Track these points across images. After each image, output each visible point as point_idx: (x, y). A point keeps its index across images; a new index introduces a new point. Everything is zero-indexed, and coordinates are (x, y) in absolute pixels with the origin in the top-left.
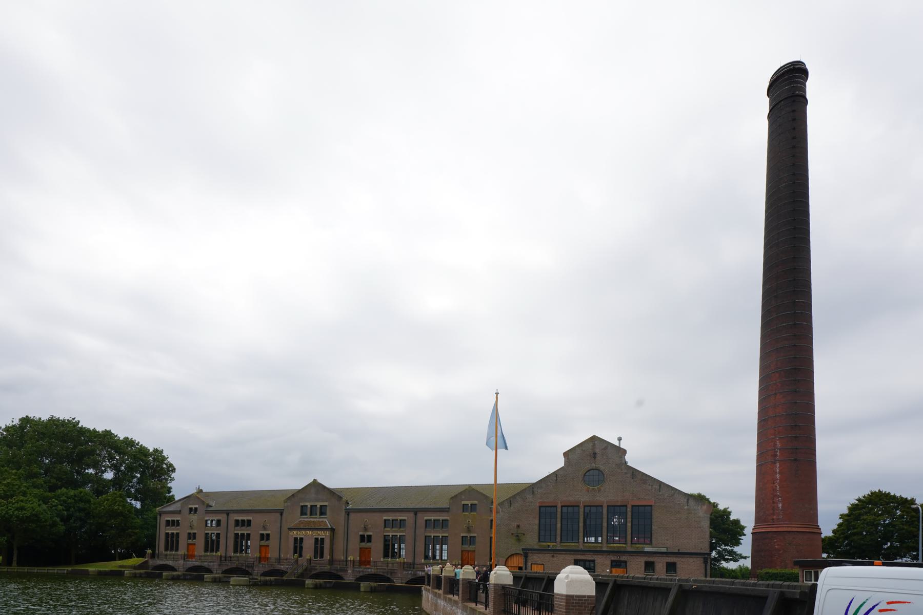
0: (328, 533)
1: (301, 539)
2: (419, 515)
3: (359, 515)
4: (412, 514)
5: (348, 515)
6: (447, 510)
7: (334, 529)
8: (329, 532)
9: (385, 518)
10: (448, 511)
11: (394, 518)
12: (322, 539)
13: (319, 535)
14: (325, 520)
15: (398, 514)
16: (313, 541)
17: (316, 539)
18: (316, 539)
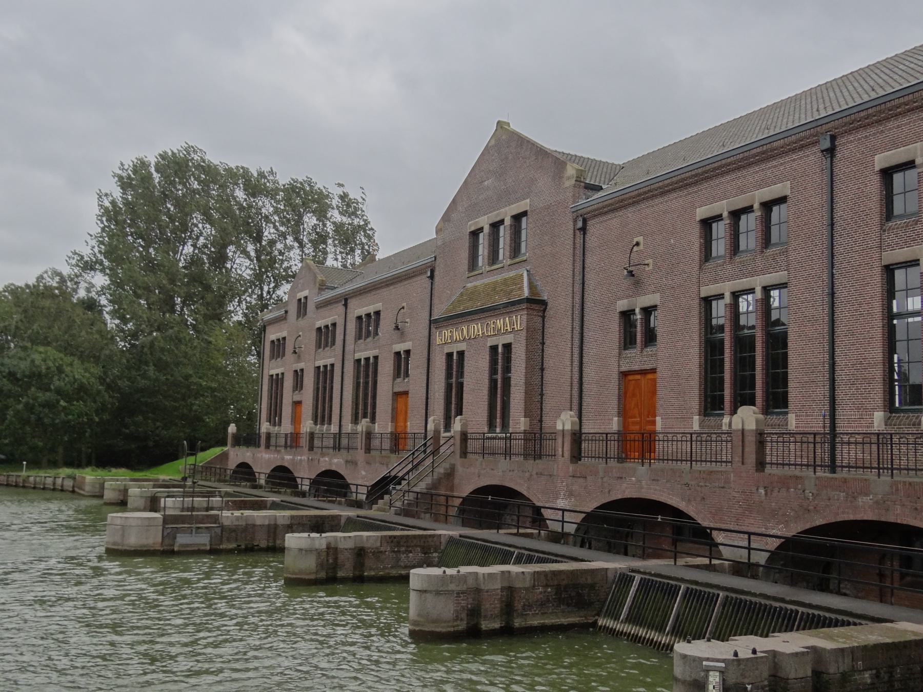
0: (519, 320)
1: (461, 354)
2: (848, 148)
3: (614, 221)
4: (812, 159)
5: (584, 230)
7: (544, 303)
8: (525, 317)
9: (703, 212)
11: (739, 202)
12: (508, 347)
13: (498, 333)
15: (752, 175)
16: (484, 362)
17: (494, 349)
18: (494, 349)
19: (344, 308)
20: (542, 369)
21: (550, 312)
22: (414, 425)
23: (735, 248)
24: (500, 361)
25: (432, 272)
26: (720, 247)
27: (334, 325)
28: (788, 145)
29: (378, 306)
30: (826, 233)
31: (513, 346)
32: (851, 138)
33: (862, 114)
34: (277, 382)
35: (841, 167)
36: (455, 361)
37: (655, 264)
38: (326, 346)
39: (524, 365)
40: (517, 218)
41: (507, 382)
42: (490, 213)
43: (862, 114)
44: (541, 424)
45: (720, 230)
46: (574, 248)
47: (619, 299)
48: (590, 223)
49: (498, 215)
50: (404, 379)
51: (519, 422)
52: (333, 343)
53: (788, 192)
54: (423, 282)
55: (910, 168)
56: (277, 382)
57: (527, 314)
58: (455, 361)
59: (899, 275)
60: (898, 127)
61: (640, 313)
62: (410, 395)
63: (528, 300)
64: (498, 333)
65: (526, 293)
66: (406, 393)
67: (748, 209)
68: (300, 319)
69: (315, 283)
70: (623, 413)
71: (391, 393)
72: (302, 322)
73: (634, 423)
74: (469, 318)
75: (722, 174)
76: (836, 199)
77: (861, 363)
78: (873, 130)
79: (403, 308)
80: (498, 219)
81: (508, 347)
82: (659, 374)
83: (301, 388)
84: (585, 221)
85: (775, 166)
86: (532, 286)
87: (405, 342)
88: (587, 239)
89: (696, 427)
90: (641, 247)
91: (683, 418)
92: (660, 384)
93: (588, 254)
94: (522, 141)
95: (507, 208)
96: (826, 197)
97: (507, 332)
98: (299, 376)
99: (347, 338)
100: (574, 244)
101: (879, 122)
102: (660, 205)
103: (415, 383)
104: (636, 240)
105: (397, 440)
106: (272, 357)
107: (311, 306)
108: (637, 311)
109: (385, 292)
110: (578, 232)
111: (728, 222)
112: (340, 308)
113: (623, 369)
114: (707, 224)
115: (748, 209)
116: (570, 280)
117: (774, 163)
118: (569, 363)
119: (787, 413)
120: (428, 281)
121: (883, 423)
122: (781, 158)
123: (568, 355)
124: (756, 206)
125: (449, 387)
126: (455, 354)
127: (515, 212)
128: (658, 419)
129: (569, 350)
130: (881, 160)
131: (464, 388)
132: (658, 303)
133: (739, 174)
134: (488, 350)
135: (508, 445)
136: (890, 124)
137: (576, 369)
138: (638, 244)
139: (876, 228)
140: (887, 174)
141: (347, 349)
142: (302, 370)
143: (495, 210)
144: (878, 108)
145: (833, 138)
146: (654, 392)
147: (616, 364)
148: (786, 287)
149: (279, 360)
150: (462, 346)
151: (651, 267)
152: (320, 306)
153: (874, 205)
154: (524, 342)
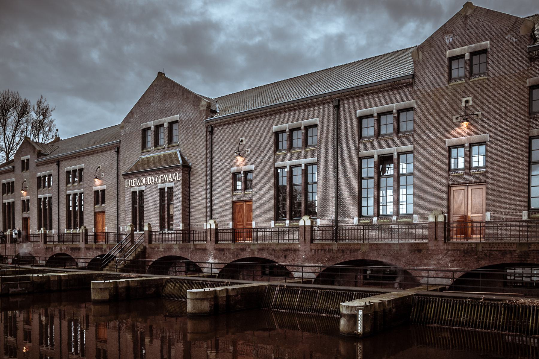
0: (177, 176)
1: (141, 192)
2: (346, 106)
3: (229, 129)
5: (212, 132)
7: (190, 167)
8: (181, 174)
9: (275, 128)
10: (412, 85)
11: (295, 124)
12: (171, 189)
14: (174, 151)
16: (156, 196)
17: (162, 190)
18: (162, 190)
19: (57, 166)
20: (189, 200)
23: (291, 147)
26: (284, 144)
28: (319, 102)
29: (82, 166)
31: (174, 188)
35: (342, 114)
39: (181, 198)
40: (171, 124)
42: (155, 120)
44: (189, 227)
45: (284, 138)
46: (206, 141)
47: (232, 167)
48: (215, 129)
49: (160, 121)
50: (101, 205)
51: (178, 225)
54: (113, 153)
55: (371, 117)
57: (182, 173)
59: (364, 162)
61: (243, 174)
62: (106, 213)
64: (165, 182)
65: (181, 163)
66: (104, 212)
67: (299, 129)
68: (24, 172)
69: (34, 152)
70: (234, 220)
72: (25, 174)
73: (240, 225)
77: (349, 197)
80: (160, 123)
83: (28, 210)
85: (312, 111)
89: (273, 226)
90: (244, 142)
91: (266, 222)
92: (254, 206)
93: (214, 145)
97: (170, 182)
99: (60, 182)
100: (206, 139)
101: (359, 96)
103: (110, 207)
104: (241, 139)
107: (32, 164)
108: (242, 172)
109: (87, 158)
111: (288, 134)
112: (55, 166)
113: (234, 200)
115: (299, 129)
116: (204, 157)
117: (311, 109)
118: (204, 197)
119: (316, 219)
121: (357, 222)
122: (315, 107)
123: (204, 193)
126: (138, 192)
127: (170, 121)
128: (254, 223)
129: (204, 191)
130: (359, 113)
133: (294, 112)
134: (159, 190)
136: (363, 98)
137: (209, 200)
138: (242, 141)
139: (357, 142)
140: (361, 119)
141: (61, 189)
143: (158, 119)
145: (339, 101)
148: (316, 164)
150: (143, 188)
151: (249, 152)
154: (180, 187)
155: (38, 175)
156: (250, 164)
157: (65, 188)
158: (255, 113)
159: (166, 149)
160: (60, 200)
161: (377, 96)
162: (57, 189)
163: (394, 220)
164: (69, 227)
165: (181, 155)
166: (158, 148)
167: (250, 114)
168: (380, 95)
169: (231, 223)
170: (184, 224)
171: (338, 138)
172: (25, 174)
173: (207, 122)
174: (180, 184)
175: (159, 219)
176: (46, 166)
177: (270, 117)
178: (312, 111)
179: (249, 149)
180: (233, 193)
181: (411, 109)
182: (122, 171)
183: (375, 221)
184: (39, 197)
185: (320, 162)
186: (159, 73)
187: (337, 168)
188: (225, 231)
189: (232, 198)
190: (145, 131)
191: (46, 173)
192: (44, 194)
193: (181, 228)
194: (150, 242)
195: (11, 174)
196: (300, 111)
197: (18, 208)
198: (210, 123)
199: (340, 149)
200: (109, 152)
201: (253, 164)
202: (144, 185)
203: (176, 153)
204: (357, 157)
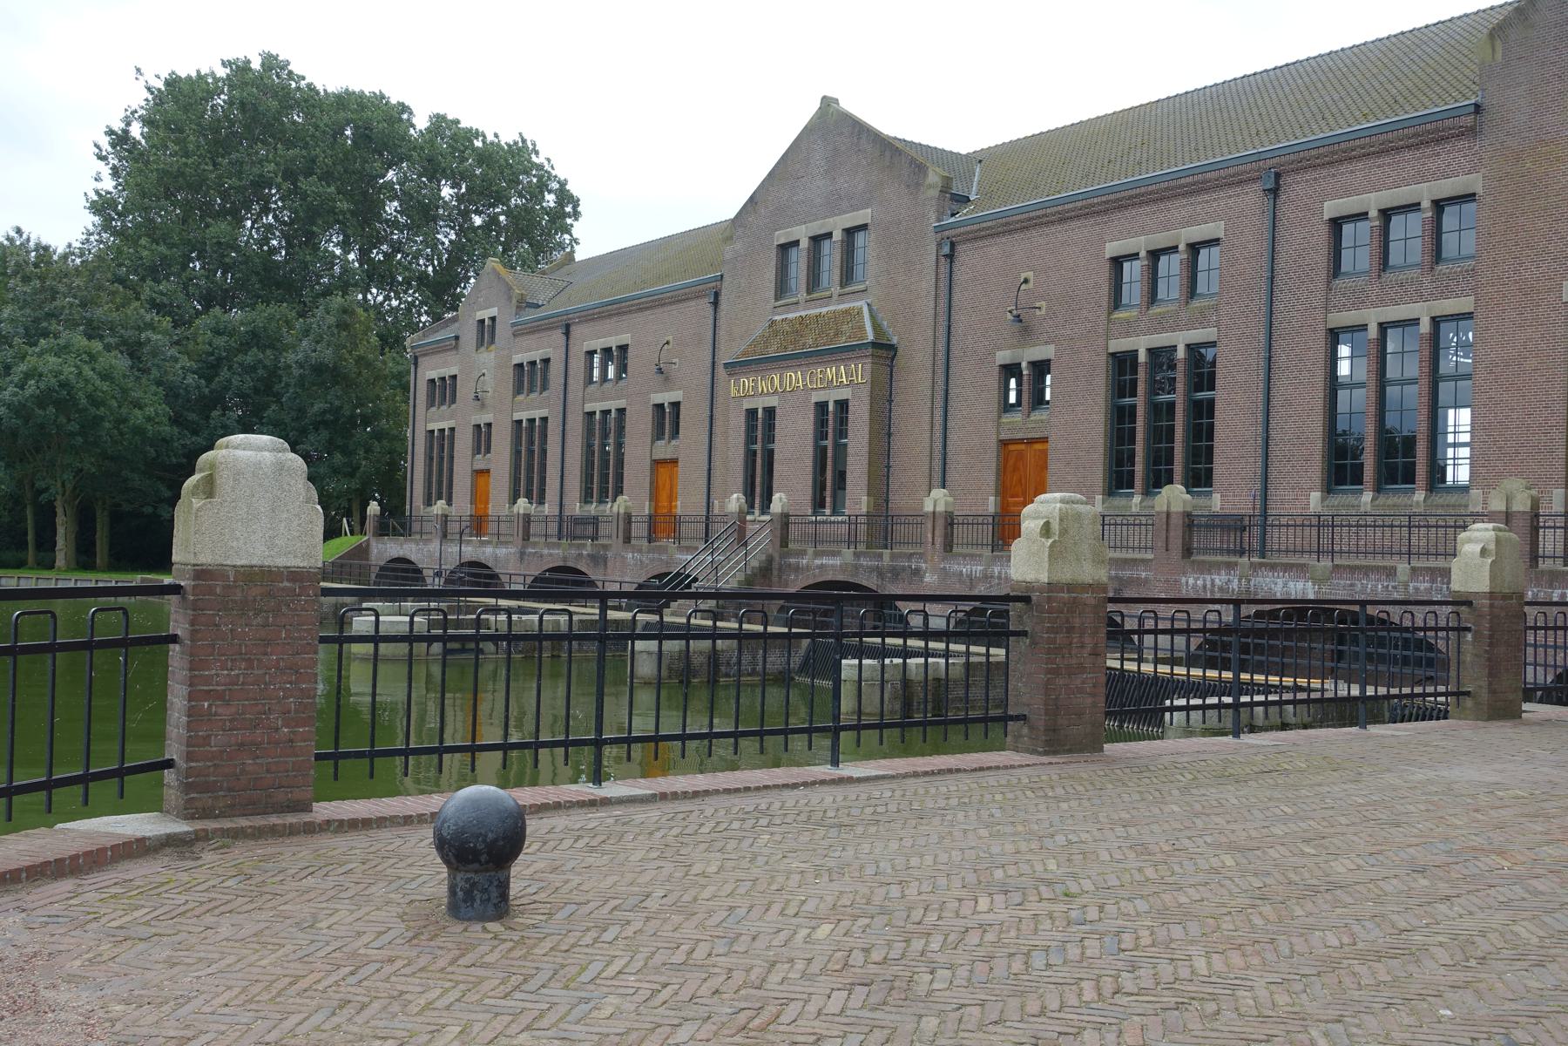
1: (770, 412)
2: (1297, 189)
4: (1251, 198)
5: (951, 257)
6: (1468, 121)
7: (892, 348)
8: (868, 367)
9: (1113, 248)
10: (1472, 132)
11: (1160, 240)
12: (843, 405)
16: (807, 423)
17: (821, 407)
18: (821, 407)
20: (889, 435)
21: (900, 361)
22: (688, 502)
23: (1152, 297)
24: (831, 422)
25: (717, 295)
27: (546, 361)
29: (625, 338)
30: (1265, 286)
32: (1298, 178)
33: (1313, 153)
34: (442, 443)
36: (760, 421)
37: (1049, 308)
38: (531, 391)
39: (867, 429)
40: (850, 232)
41: (841, 450)
43: (1313, 153)
46: (937, 279)
51: (858, 499)
52: (544, 387)
53: (1221, 235)
54: (704, 306)
56: (442, 443)
58: (760, 421)
60: (1352, 172)
63: (874, 345)
65: (871, 337)
66: (674, 462)
67: (1173, 249)
68: (483, 349)
69: (510, 298)
71: (648, 462)
74: (784, 364)
75: (1141, 204)
76: (1278, 248)
78: (1324, 172)
79: (668, 343)
81: (843, 405)
82: (1051, 445)
83: (488, 450)
84: (953, 245)
85: (1207, 202)
86: (877, 327)
87: (672, 390)
88: (955, 269)
90: (1031, 285)
94: (859, 130)
95: (837, 218)
96: (1266, 245)
97: (841, 386)
98: (483, 437)
99: (571, 381)
101: (1330, 163)
102: (1058, 233)
103: (689, 445)
104: (1023, 276)
105: (662, 525)
106: (431, 403)
107: (502, 331)
109: (638, 318)
110: (943, 259)
112: (558, 336)
113: (1003, 436)
114: (1117, 262)
116: (931, 321)
117: (1206, 197)
118: (927, 427)
120: (710, 309)
123: (927, 418)
124: (1182, 247)
125: (750, 456)
126: (760, 411)
127: (848, 225)
129: (927, 410)
130: (1331, 208)
131: (776, 457)
132: (1052, 357)
135: (853, 532)
136: (1342, 169)
138: (1026, 281)
139: (1322, 286)
140: (1336, 224)
141: (570, 397)
142: (489, 425)
144: (1331, 148)
145: (1278, 176)
146: (1044, 466)
147: (994, 430)
149: (444, 408)
150: (772, 401)
151: (1043, 312)
152: (519, 331)
153: (1321, 257)
154: (867, 400)
155: (517, 359)
156: (1047, 343)
157: (581, 394)
158: (1060, 208)
159: (835, 297)
160: (568, 427)
161: (1380, 161)
162: (562, 396)
163: (1418, 502)
164: (587, 497)
165: (872, 317)
166: (814, 296)
167: (1048, 211)
168: (1388, 160)
169: (992, 499)
170: (872, 499)
171: (1272, 278)
172: (485, 355)
173: (939, 230)
174: (865, 393)
175: (810, 482)
176: (537, 335)
177: (1099, 219)
178: (1207, 202)
179: (1044, 303)
180: (1000, 417)
181: (1470, 197)
182: (724, 357)
183: (1366, 504)
184: (517, 417)
185: (1225, 341)
186: (824, 98)
187: (1270, 358)
188: (973, 521)
189: (998, 433)
190: (785, 248)
191: (537, 355)
192: (528, 409)
193: (864, 510)
194: (784, 542)
195: (451, 356)
196: (1177, 203)
197: (464, 443)
198: (947, 233)
199: (1278, 306)
200: (693, 303)
201: (1053, 342)
202: (776, 392)
203: (860, 312)
204: (1322, 327)
